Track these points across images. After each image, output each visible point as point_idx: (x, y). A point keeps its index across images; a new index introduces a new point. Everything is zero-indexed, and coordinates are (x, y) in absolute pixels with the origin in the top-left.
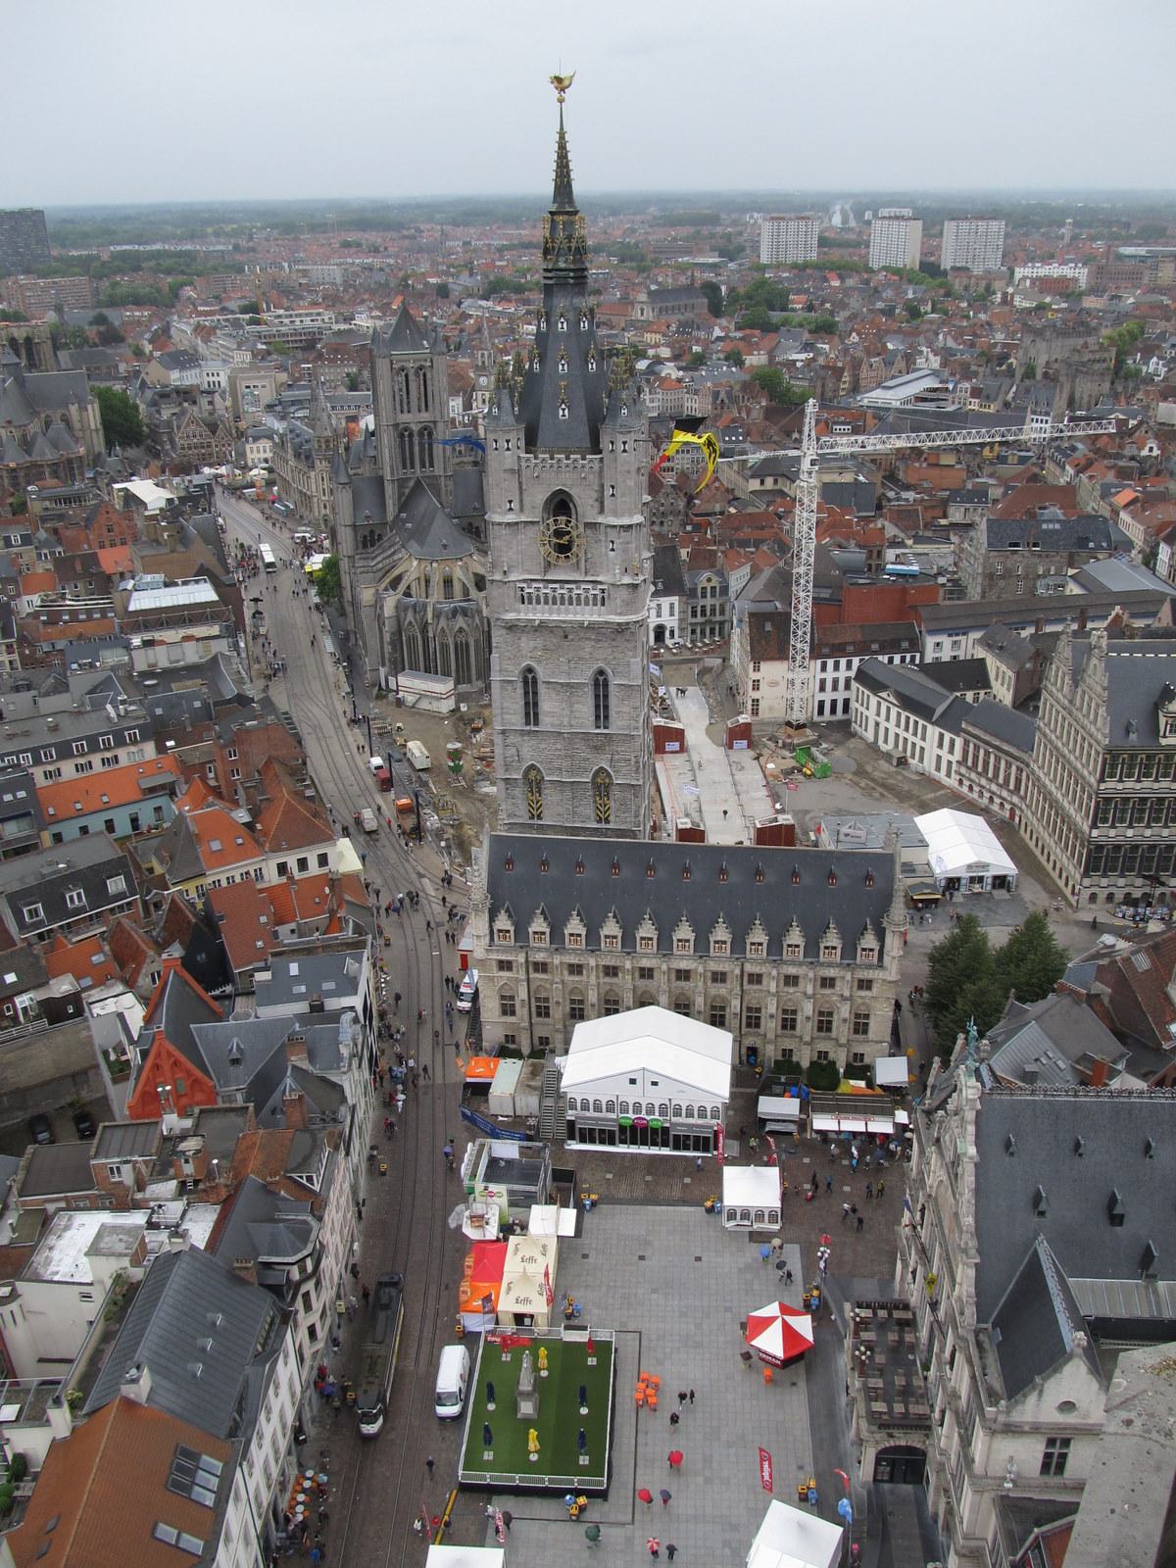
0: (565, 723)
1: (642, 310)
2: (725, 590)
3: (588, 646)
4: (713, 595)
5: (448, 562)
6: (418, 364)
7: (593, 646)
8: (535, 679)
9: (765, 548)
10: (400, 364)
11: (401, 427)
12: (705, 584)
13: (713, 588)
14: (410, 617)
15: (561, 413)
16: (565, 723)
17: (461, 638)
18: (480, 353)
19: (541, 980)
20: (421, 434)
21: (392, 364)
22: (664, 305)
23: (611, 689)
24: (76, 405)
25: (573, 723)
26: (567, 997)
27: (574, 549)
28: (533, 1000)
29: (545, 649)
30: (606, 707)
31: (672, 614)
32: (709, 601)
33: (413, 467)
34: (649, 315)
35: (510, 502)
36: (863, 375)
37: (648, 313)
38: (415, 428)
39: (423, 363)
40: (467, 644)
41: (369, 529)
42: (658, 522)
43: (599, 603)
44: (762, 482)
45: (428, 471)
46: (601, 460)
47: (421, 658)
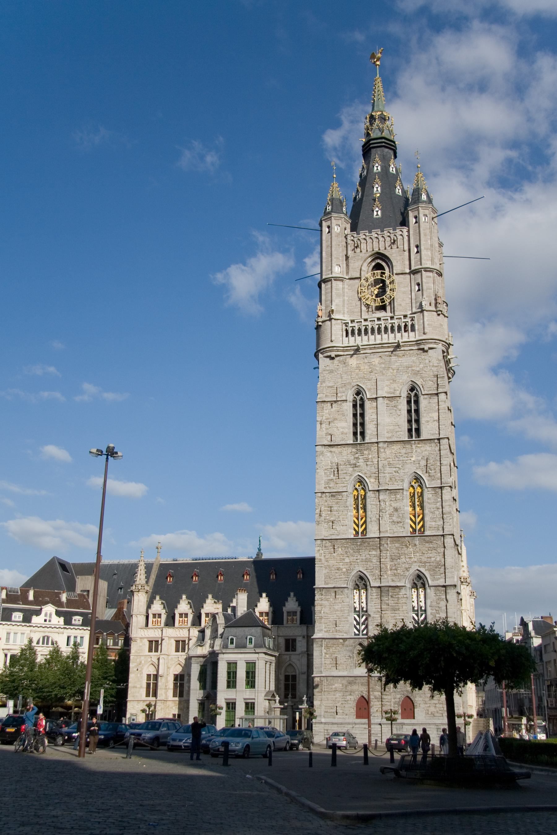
46: (408, 231)
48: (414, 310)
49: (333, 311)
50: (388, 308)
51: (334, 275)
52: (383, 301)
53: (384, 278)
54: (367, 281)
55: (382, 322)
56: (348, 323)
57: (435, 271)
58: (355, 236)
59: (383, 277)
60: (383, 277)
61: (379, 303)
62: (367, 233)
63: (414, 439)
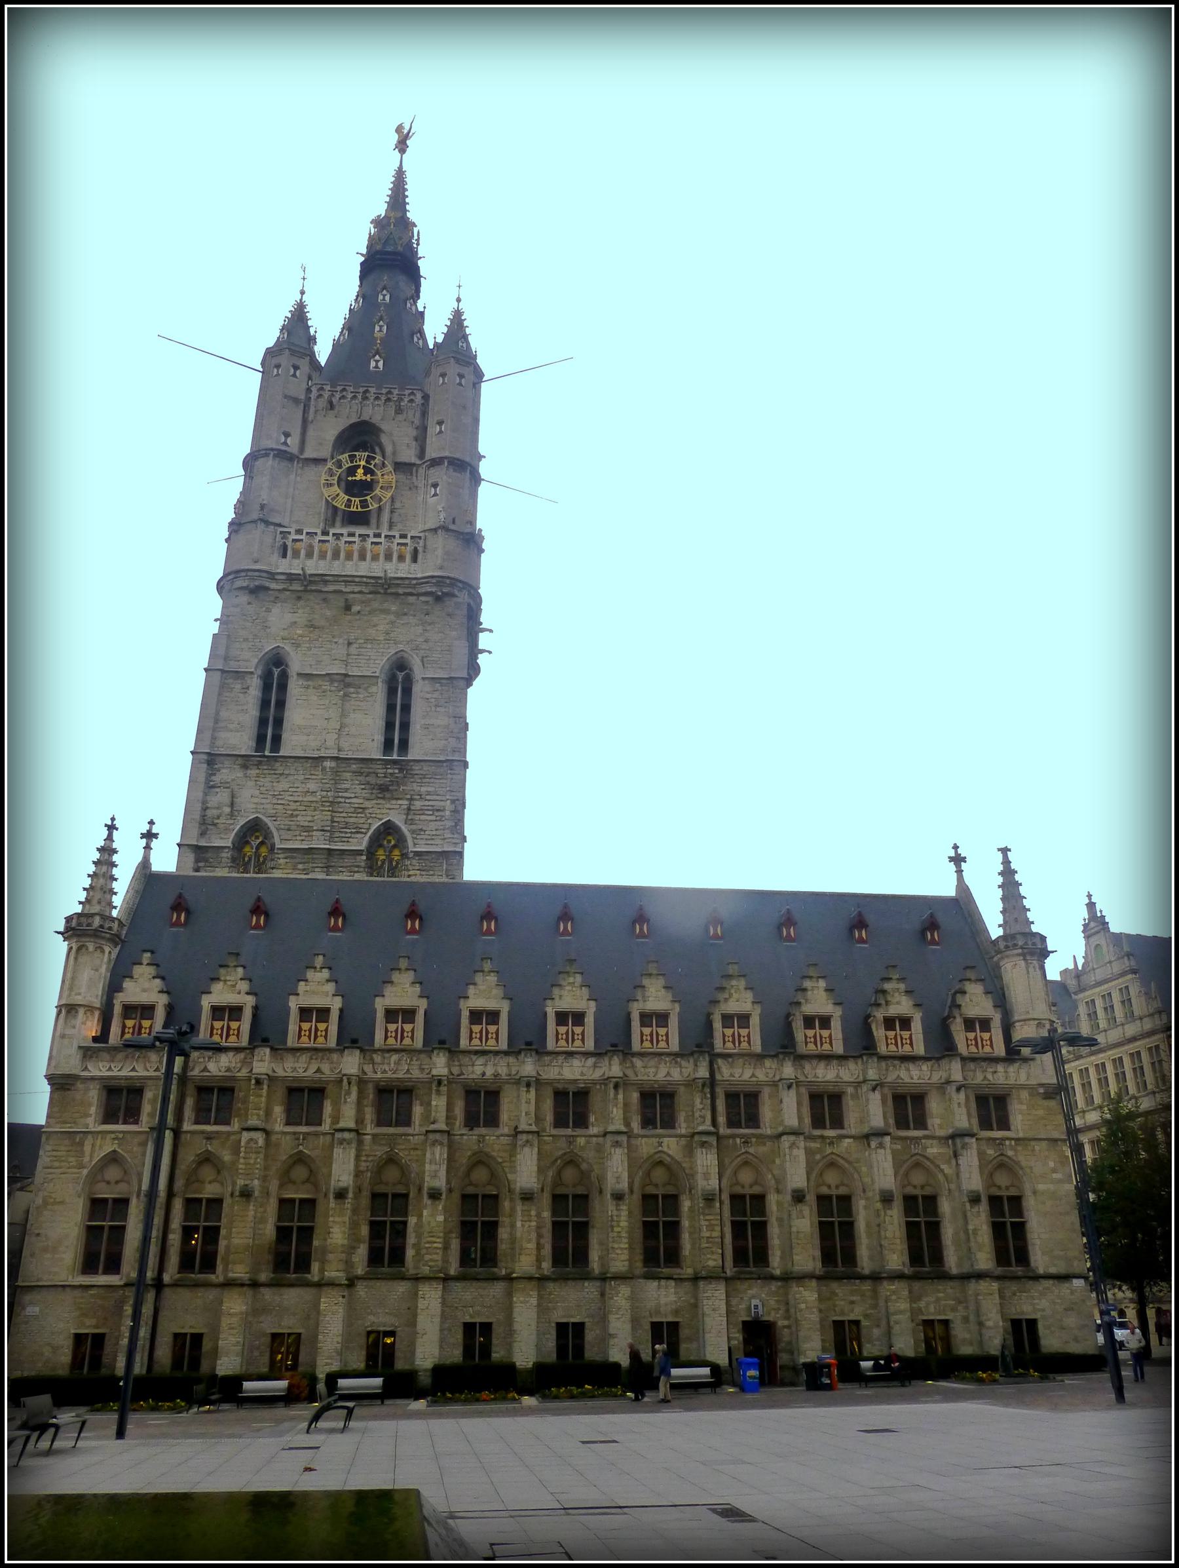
0: (330, 743)
3: (382, 623)
7: (392, 623)
8: (284, 676)
15: (373, 364)
16: (330, 743)
19: (209, 1137)
23: (418, 688)
25: (345, 744)
26: (274, 1186)
27: (378, 491)
28: (178, 1205)
29: (312, 626)
30: (405, 726)
35: (287, 435)
43: (408, 557)
46: (426, 397)
48: (421, 527)
49: (262, 507)
50: (373, 521)
51: (274, 446)
52: (364, 504)
53: (372, 467)
54: (340, 467)
55: (356, 539)
56: (289, 533)
57: (469, 468)
58: (328, 388)
59: (371, 464)
60: (371, 464)
61: (357, 508)
62: (352, 388)
63: (395, 757)
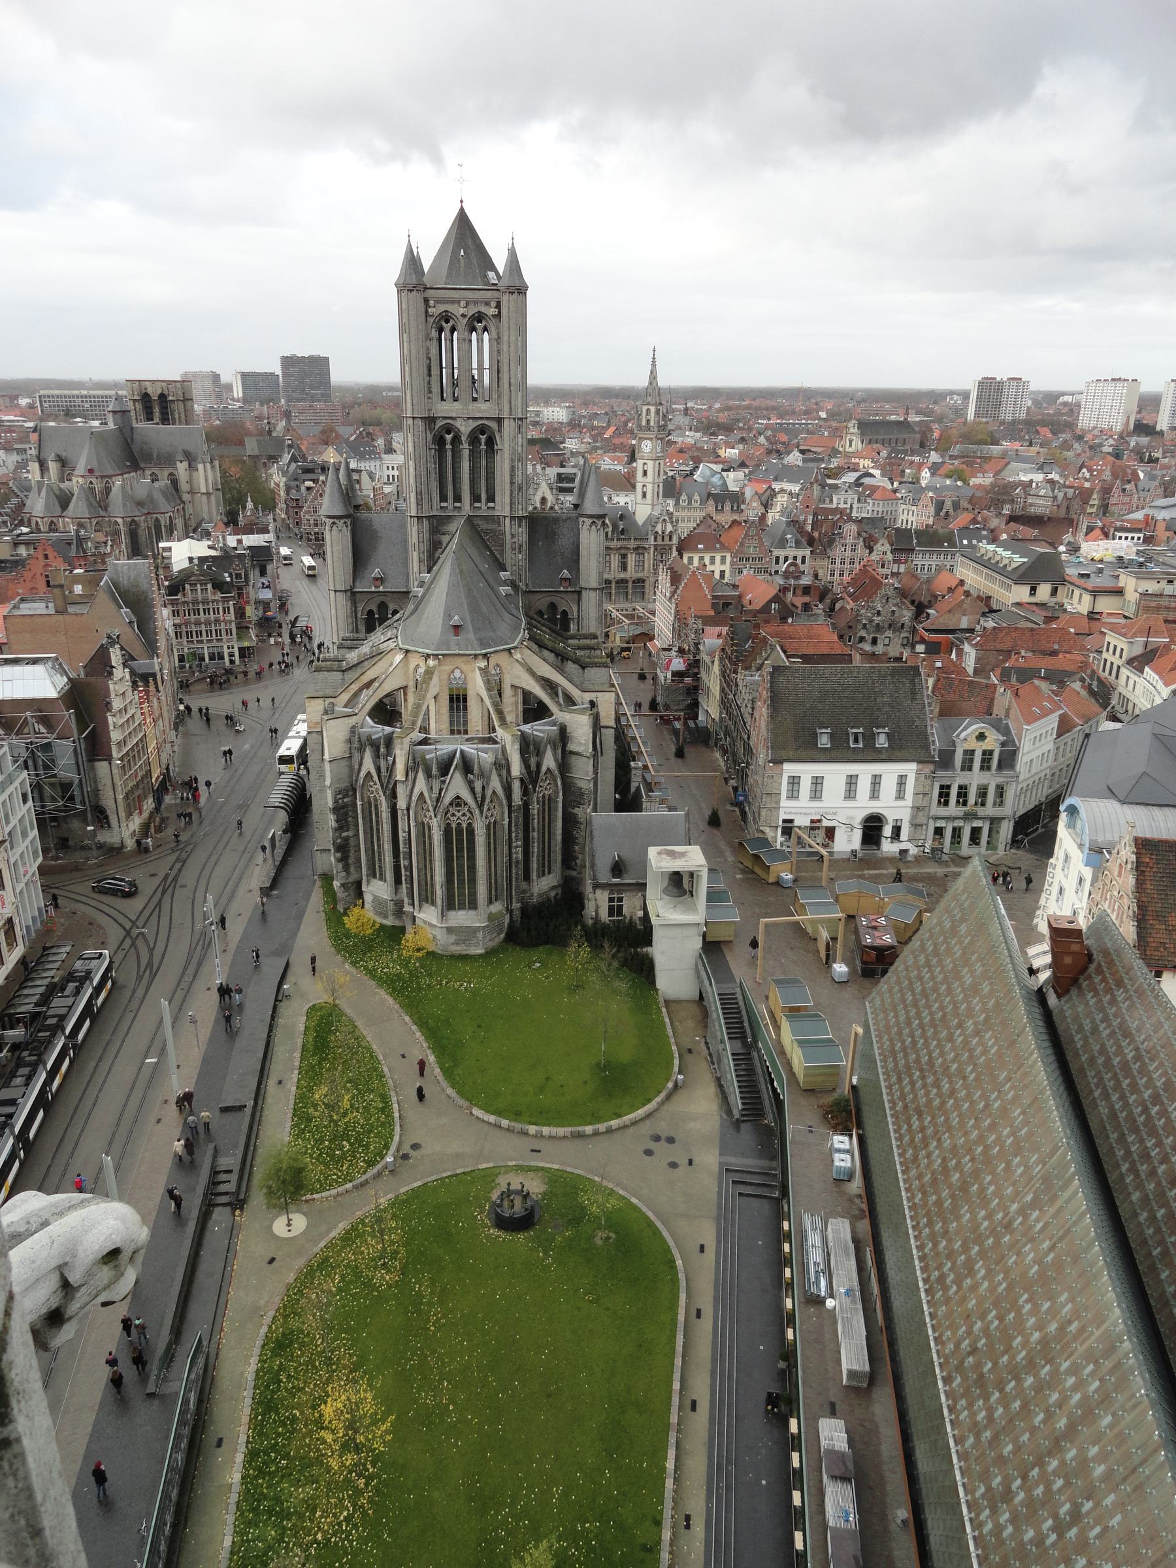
1: (851, 442)
2: (1008, 759)
4: (985, 766)
5: (459, 661)
6: (472, 310)
9: (1077, 686)
10: (441, 308)
11: (439, 424)
12: (973, 744)
13: (987, 754)
14: (368, 765)
17: (459, 818)
18: (645, 408)
20: (474, 439)
21: (426, 301)
22: (875, 437)
24: (186, 464)
31: (900, 795)
32: (975, 779)
33: (458, 498)
34: (857, 445)
36: (1113, 501)
37: (857, 445)
38: (465, 428)
39: (484, 309)
40: (471, 831)
41: (379, 599)
42: (869, 638)
44: (1033, 590)
45: (483, 507)
47: (387, 847)
